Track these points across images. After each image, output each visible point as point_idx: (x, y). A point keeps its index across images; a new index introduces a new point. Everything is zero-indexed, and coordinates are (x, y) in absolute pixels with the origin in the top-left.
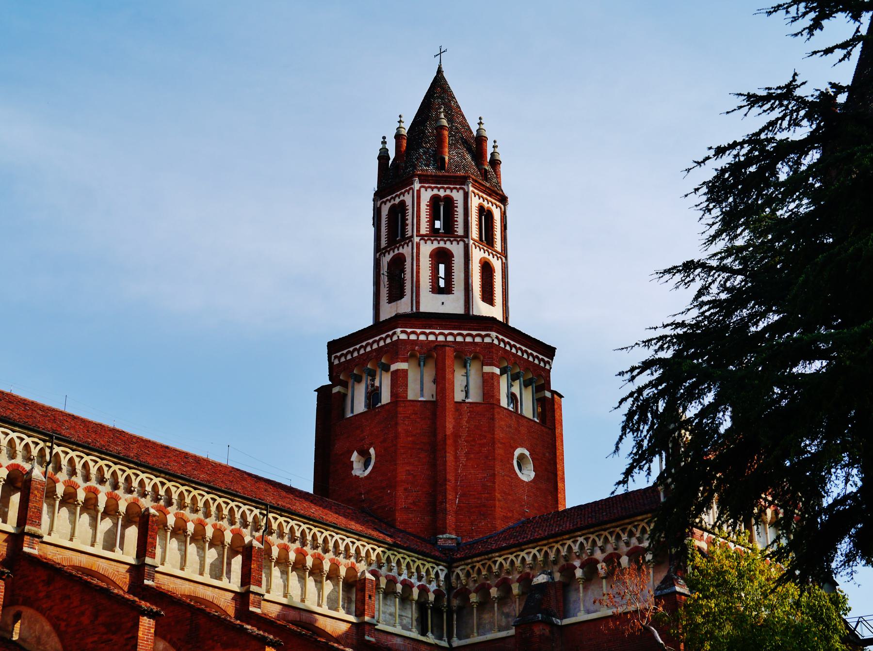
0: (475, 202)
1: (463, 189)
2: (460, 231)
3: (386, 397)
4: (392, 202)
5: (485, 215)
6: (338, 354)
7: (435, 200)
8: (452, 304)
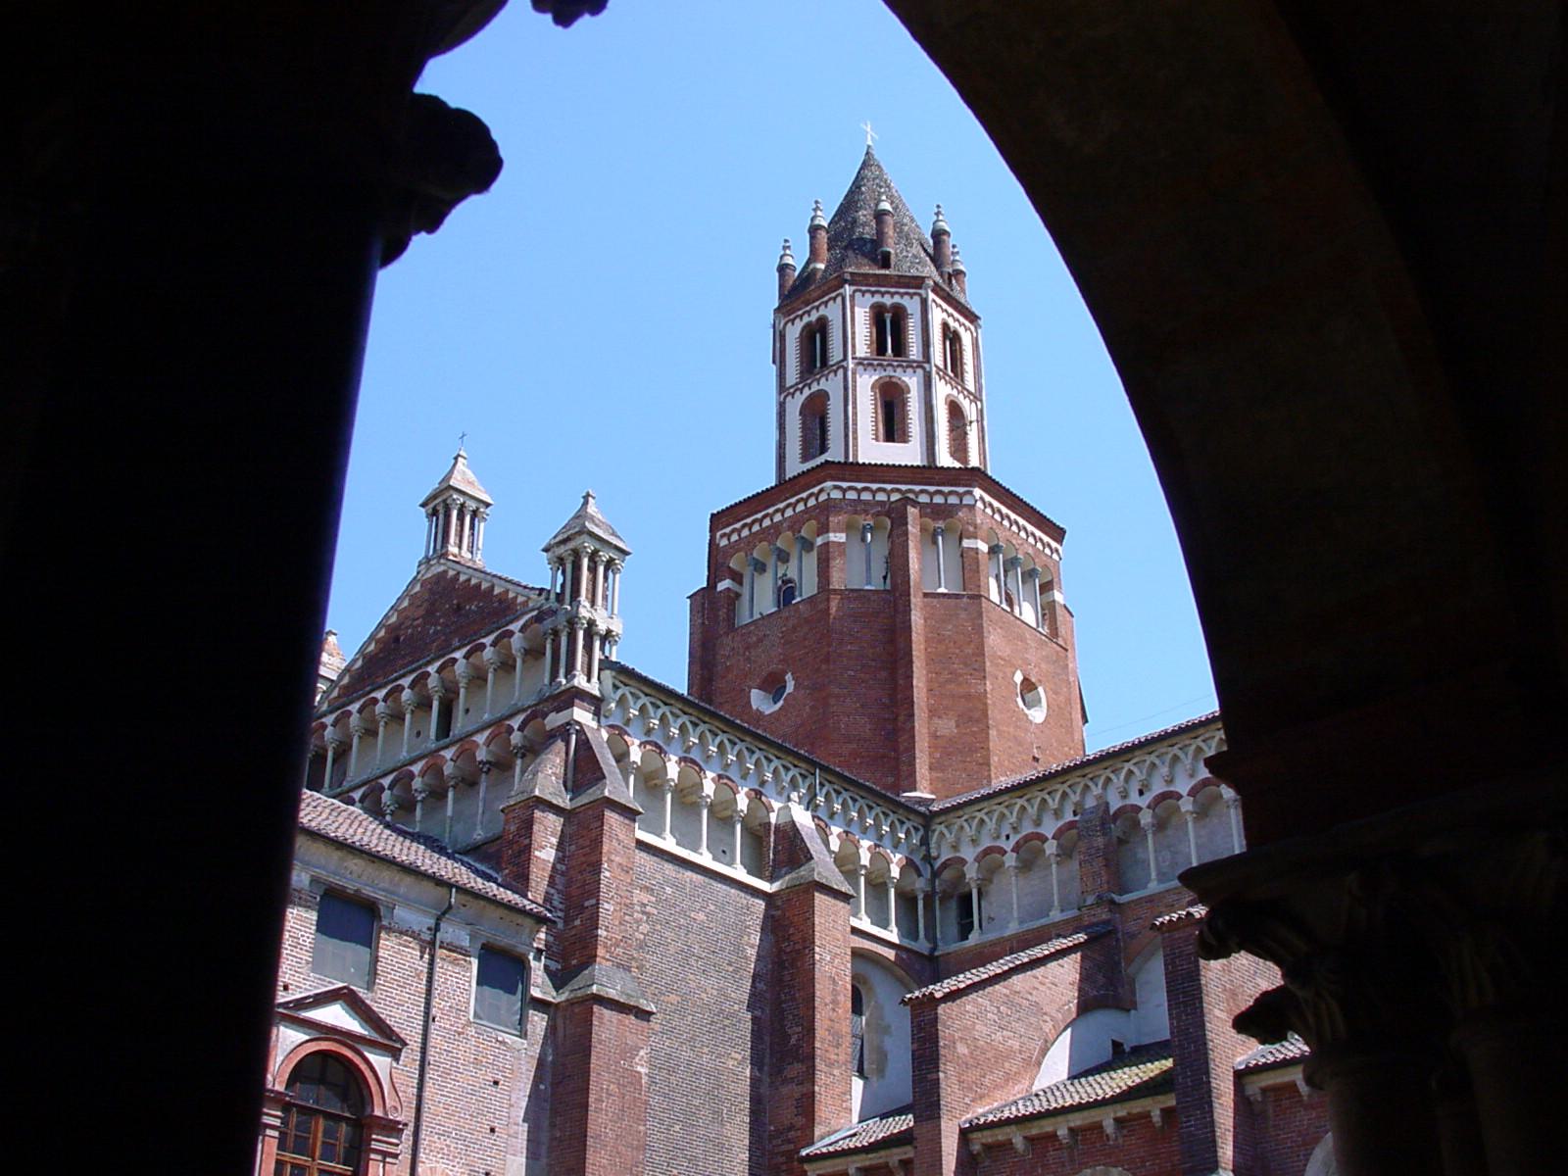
0: (938, 316)
1: (920, 295)
2: (914, 351)
3: (809, 587)
4: (806, 319)
5: (951, 337)
6: (728, 530)
7: (878, 315)
8: (907, 453)
